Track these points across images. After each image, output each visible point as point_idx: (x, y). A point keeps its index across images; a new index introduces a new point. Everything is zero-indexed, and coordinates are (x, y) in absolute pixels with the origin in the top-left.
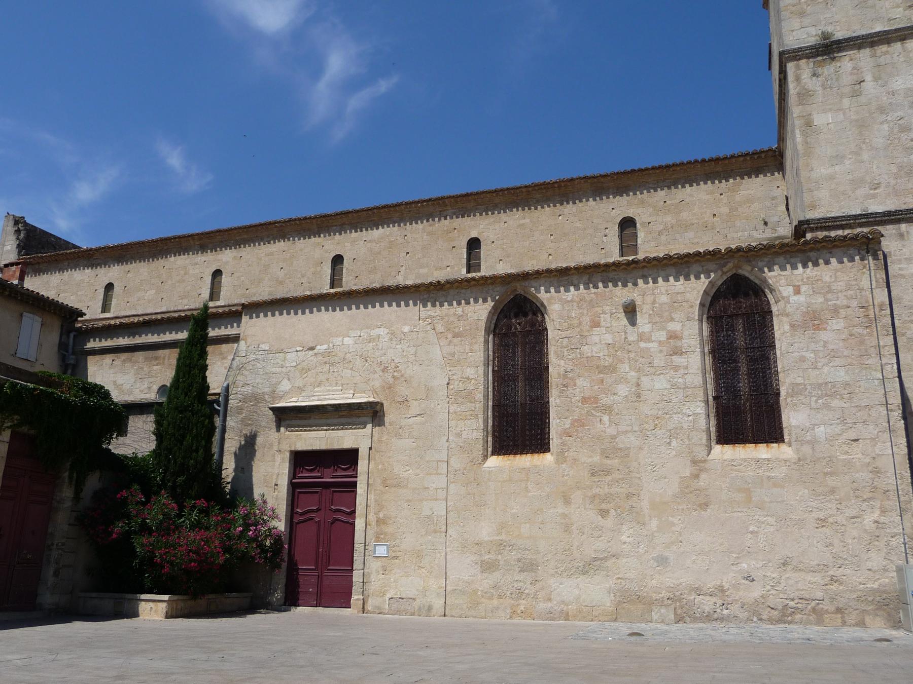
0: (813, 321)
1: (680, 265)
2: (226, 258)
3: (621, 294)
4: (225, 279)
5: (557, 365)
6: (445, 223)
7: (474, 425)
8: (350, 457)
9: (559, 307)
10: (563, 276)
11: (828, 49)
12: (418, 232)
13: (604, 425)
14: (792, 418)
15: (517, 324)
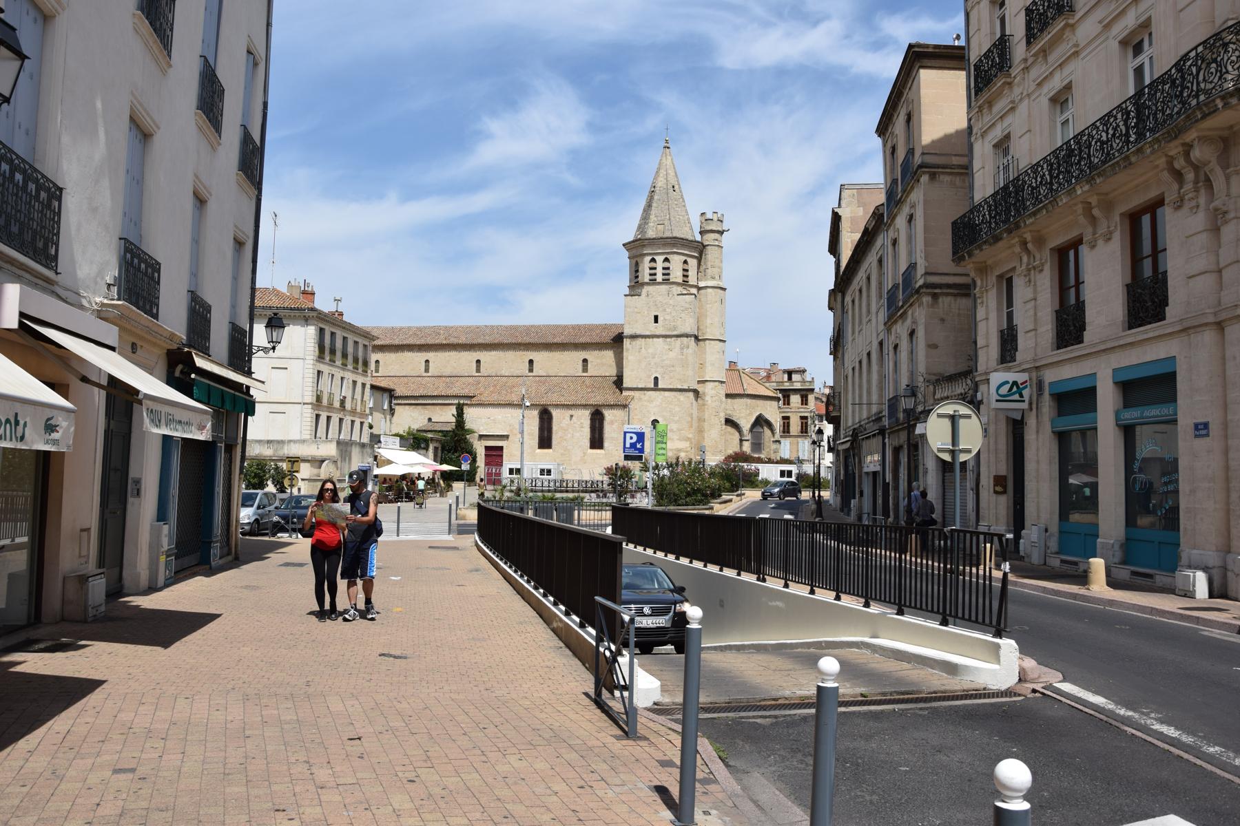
0: (612, 423)
1: (585, 406)
2: (430, 355)
3: (571, 412)
4: (431, 364)
5: (555, 428)
6: (521, 353)
7: (535, 441)
8: (501, 448)
9: (556, 413)
10: (557, 406)
11: (634, 337)
12: (510, 355)
13: (564, 443)
14: (606, 444)
15: (546, 417)
